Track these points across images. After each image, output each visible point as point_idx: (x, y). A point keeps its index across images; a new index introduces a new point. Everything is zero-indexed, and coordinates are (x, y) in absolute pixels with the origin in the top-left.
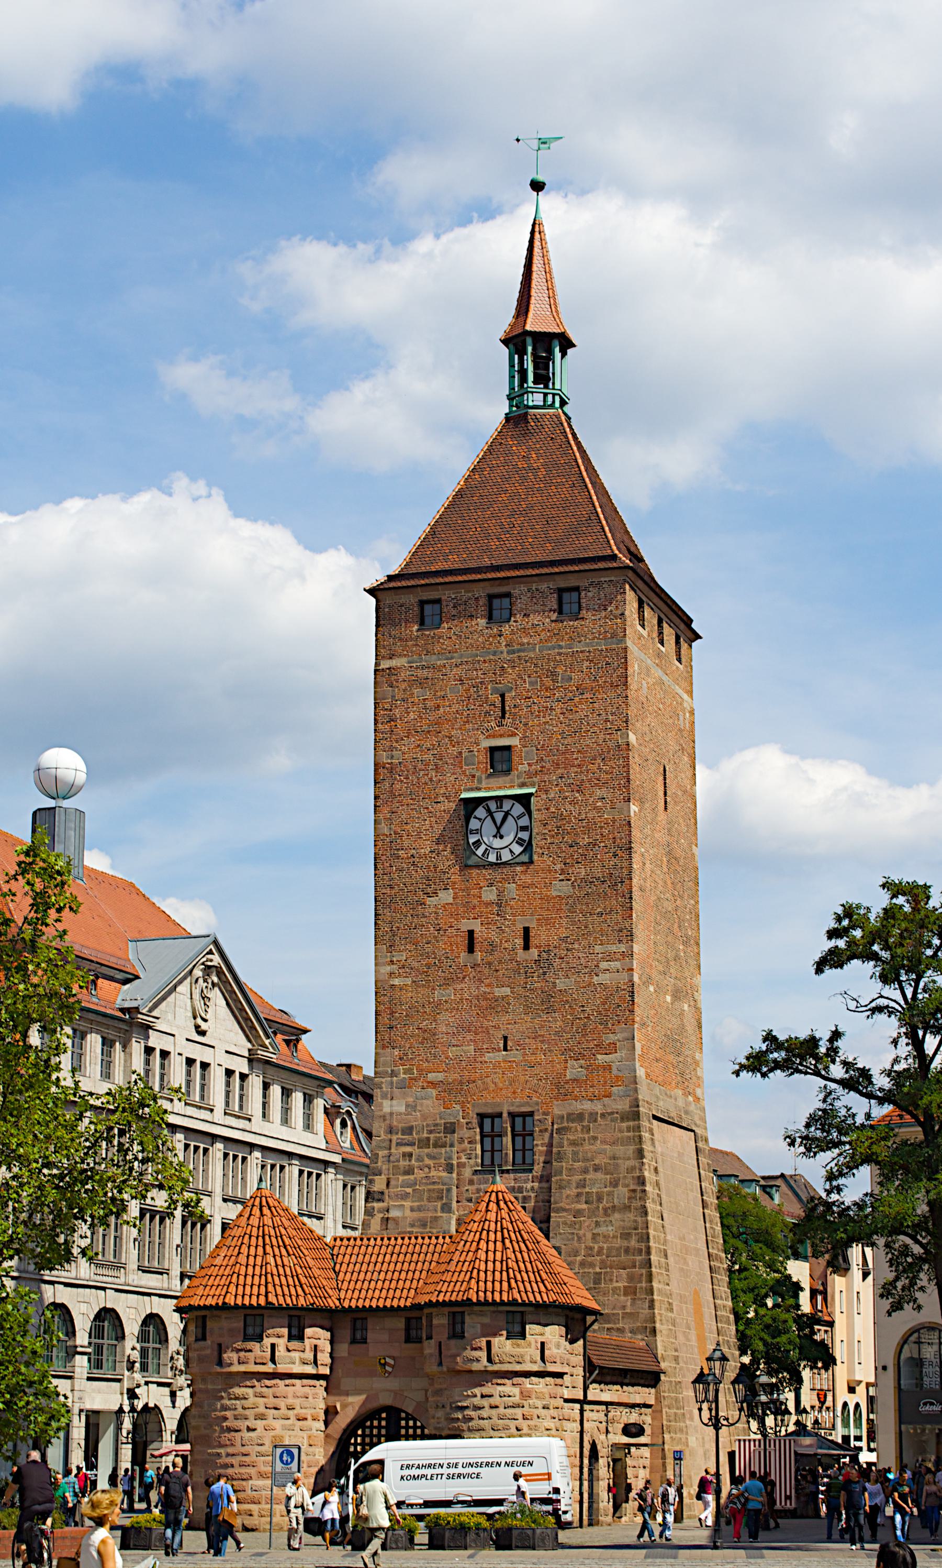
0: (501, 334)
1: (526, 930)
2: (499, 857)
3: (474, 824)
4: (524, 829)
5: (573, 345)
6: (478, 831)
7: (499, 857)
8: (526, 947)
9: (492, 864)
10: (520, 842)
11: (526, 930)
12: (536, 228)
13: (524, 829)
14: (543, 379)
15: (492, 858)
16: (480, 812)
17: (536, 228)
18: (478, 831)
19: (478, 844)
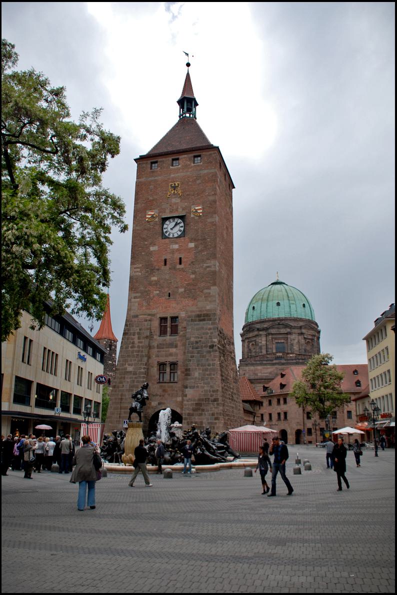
0: (177, 100)
1: (180, 259)
2: (173, 236)
3: (165, 226)
4: (181, 227)
5: (198, 105)
6: (166, 228)
7: (173, 236)
8: (180, 263)
9: (171, 238)
10: (180, 231)
11: (180, 259)
12: (188, 76)
13: (181, 227)
14: (189, 110)
15: (171, 236)
16: (167, 222)
17: (188, 76)
18: (166, 228)
19: (166, 232)
